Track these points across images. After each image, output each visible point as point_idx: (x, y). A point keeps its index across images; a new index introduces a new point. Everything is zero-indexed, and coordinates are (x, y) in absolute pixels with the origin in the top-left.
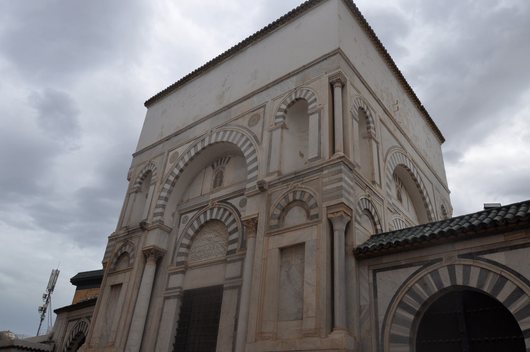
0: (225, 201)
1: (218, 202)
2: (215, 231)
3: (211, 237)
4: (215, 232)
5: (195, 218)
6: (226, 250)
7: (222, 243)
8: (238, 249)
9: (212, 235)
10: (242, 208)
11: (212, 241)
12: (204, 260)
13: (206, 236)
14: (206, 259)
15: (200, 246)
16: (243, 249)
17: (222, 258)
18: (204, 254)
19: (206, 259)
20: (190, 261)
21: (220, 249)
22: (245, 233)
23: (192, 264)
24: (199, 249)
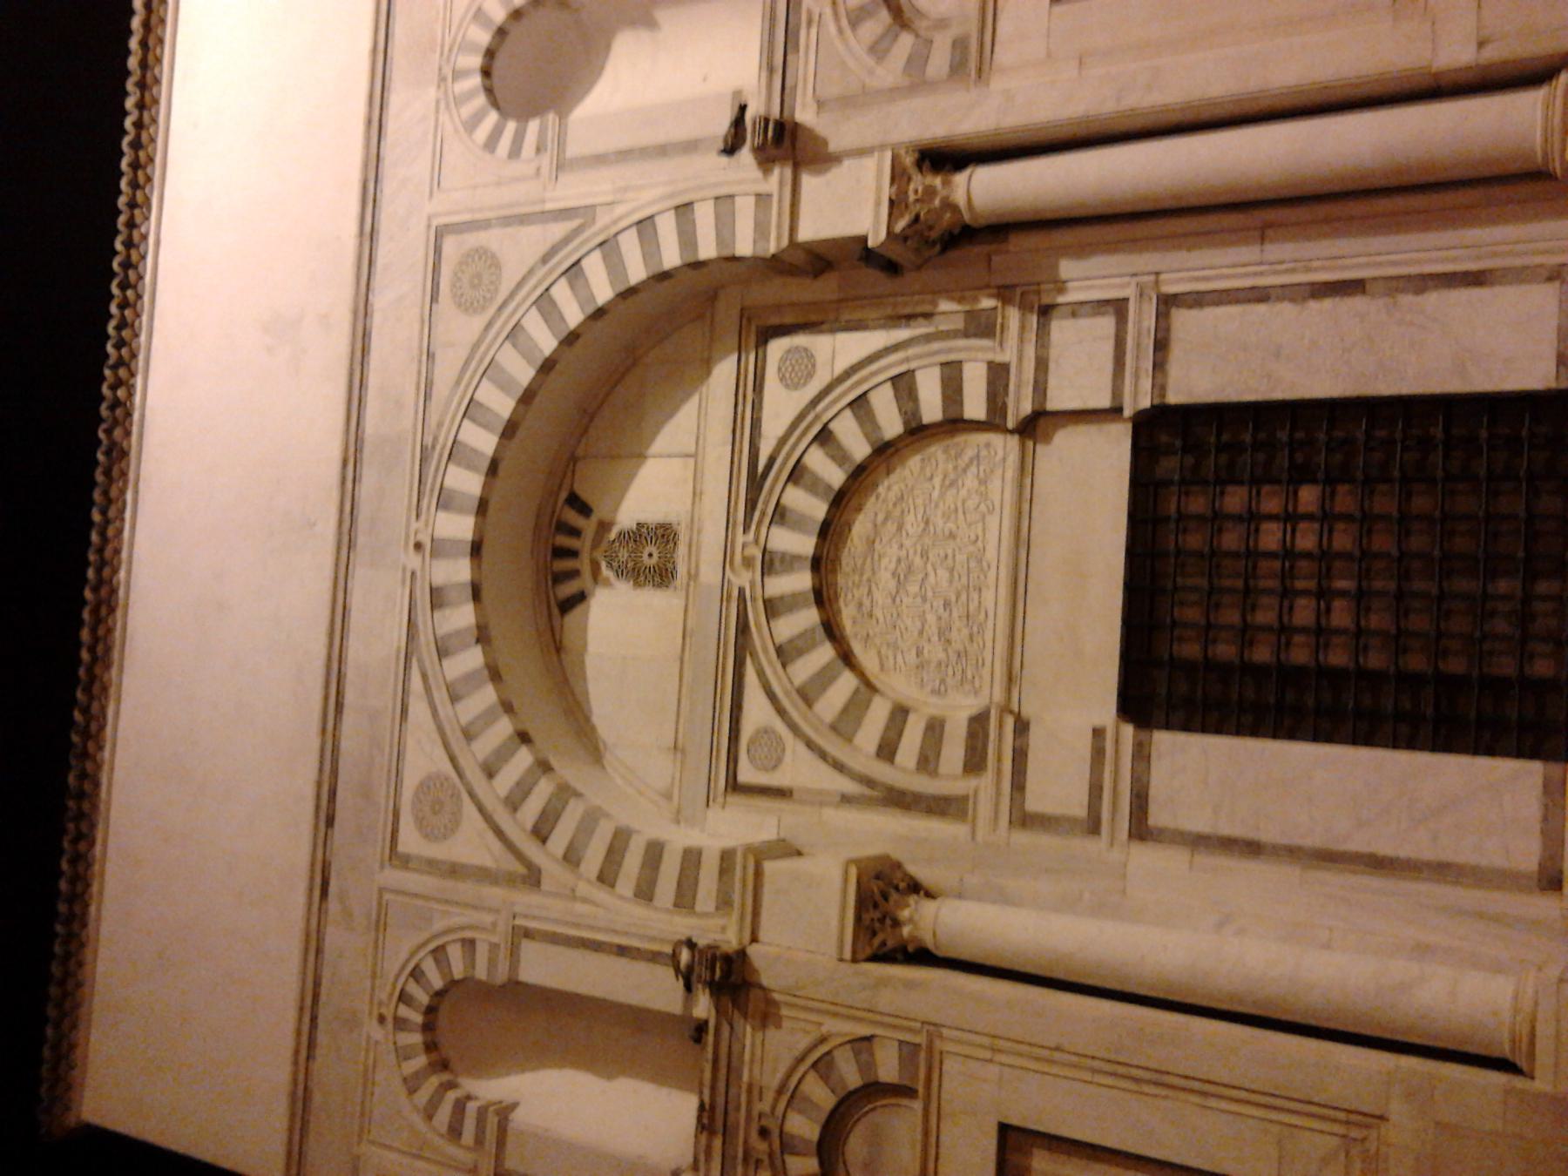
0: (756, 482)
1: (746, 529)
2: (874, 542)
3: (893, 566)
4: (877, 541)
6: (978, 456)
7: (942, 486)
8: (990, 356)
11: (915, 552)
12: (994, 599)
14: (992, 574)
15: (921, 633)
16: (999, 320)
18: (964, 597)
19: (992, 574)
20: (976, 693)
21: (963, 492)
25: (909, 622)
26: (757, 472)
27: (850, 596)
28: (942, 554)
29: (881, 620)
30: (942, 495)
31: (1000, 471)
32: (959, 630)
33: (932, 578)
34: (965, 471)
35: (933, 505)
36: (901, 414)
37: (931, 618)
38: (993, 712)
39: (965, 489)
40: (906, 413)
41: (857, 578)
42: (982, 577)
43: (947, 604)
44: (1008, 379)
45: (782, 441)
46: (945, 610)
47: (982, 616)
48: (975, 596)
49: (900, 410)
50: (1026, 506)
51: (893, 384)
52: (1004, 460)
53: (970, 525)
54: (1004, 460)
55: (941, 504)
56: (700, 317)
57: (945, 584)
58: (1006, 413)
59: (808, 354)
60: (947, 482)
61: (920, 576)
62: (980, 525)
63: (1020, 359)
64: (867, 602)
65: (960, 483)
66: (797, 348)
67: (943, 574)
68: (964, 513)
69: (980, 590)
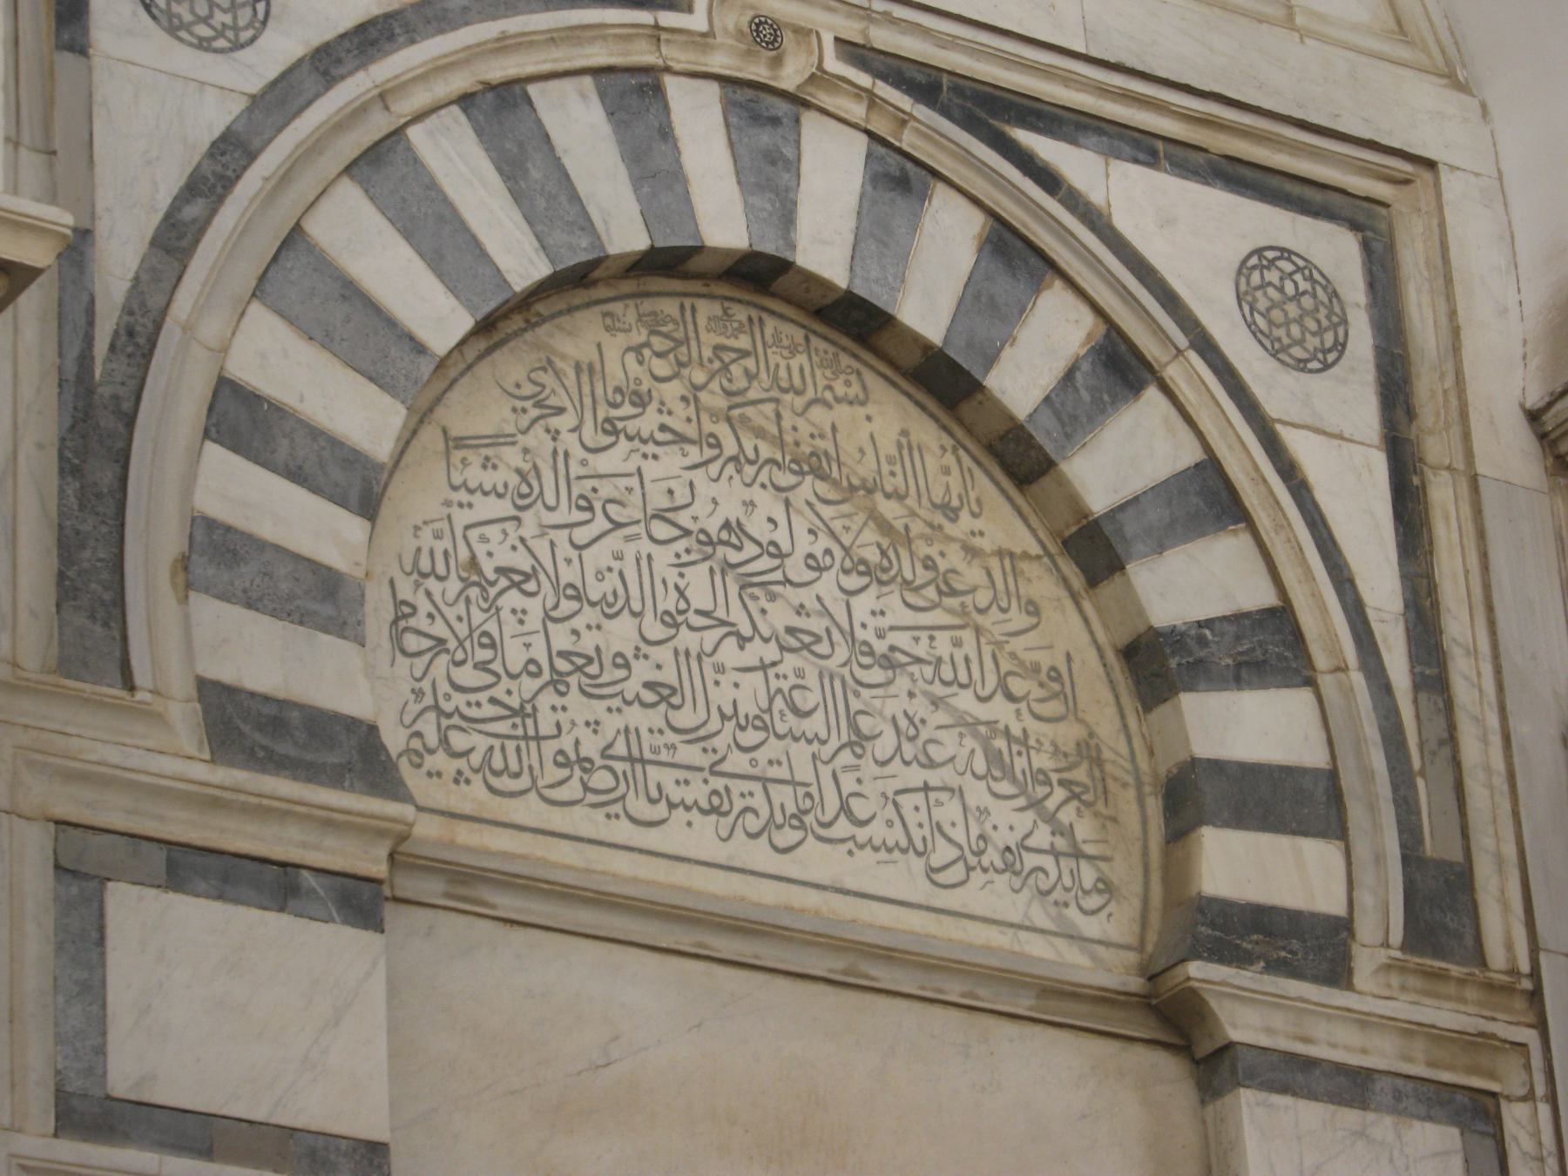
1: (853, 51)
2: (824, 477)
4: (823, 488)
5: (441, 68)
6: (1078, 854)
8: (1366, 929)
9: (769, 505)
10: (1291, 380)
11: (800, 610)
13: (650, 469)
14: (759, 855)
17: (1037, 947)
18: (690, 754)
19: (759, 855)
21: (977, 793)
22: (1416, 763)
23: (466, 835)
24: (561, 640)
25: (598, 556)
26: (1008, 122)
27: (662, 368)
28: (807, 700)
29: (602, 463)
30: (968, 724)
31: (1041, 920)
32: (594, 725)
33: (730, 653)
34: (1035, 804)
35: (939, 689)
36: (1200, 624)
37: (621, 634)
38: (392, 808)
39: (989, 801)
40: (1202, 641)
41: (713, 399)
42: (753, 823)
43: (663, 694)
44: (1316, 979)
45: (1096, 220)
46: (649, 685)
47: (639, 806)
48: (697, 792)
49: (1208, 623)
50: (954, 990)
51: (1270, 612)
52: (1074, 937)
53: (893, 800)
54: (1074, 937)
55: (942, 717)
56: (1401, 29)
57: (722, 696)
58: (1222, 960)
59: (1328, 357)
60: (1000, 743)
61: (737, 615)
62: (896, 835)
63: (1364, 1021)
64: (648, 422)
65: (1005, 787)
66: (1344, 321)
67: (750, 694)
68: (926, 788)
69: (714, 810)
